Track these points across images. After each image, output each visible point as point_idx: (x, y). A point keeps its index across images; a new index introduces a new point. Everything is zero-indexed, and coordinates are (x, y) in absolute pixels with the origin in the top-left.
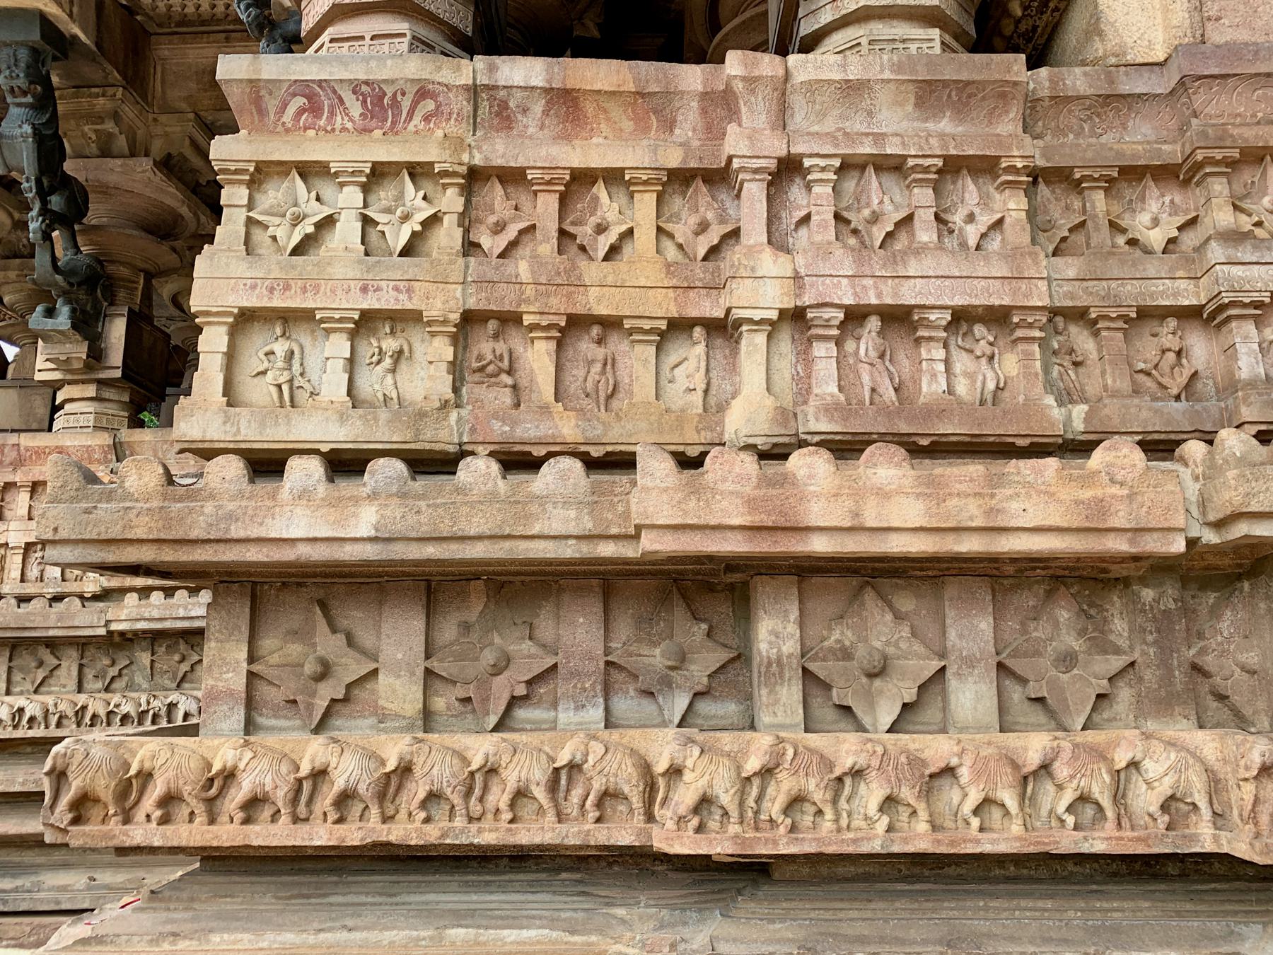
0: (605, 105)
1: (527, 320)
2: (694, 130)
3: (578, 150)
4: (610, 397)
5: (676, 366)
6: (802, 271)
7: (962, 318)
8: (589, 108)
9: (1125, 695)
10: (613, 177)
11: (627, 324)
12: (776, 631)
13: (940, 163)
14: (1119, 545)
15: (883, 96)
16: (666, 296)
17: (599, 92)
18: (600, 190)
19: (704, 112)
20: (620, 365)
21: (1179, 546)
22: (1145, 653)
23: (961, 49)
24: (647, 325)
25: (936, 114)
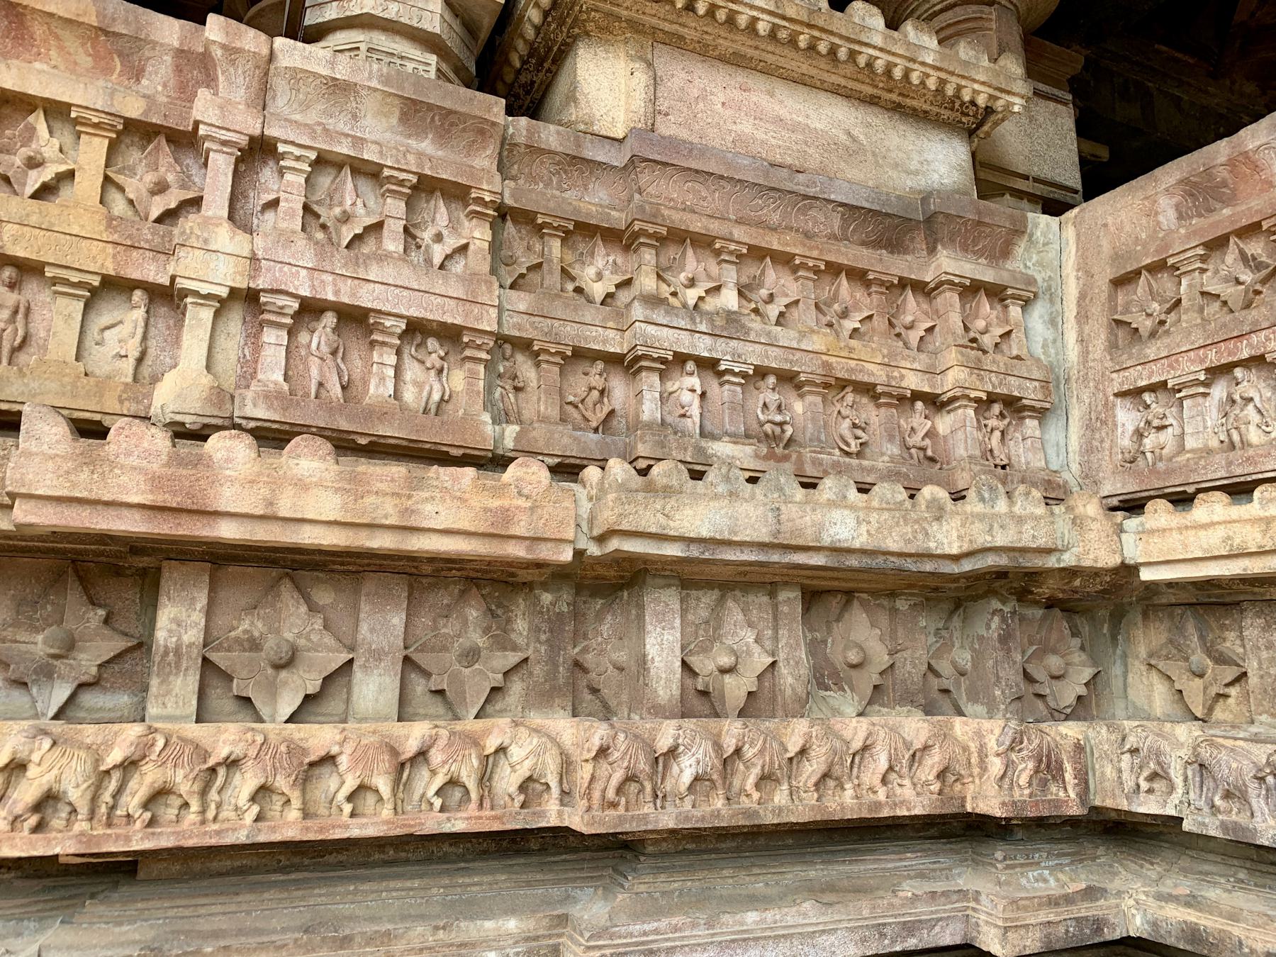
0: (59, 32)
2: (165, 86)
3: (14, 71)
4: (15, 350)
5: (108, 328)
6: (260, 254)
7: (416, 329)
8: (38, 30)
9: (517, 687)
10: (57, 111)
11: (49, 272)
12: (179, 619)
13: (415, 180)
14: (517, 551)
15: (369, 104)
16: (104, 250)
17: (51, 15)
18: (39, 121)
19: (178, 70)
20: (36, 316)
21: (567, 555)
22: (536, 651)
23: (457, 80)
24: (75, 277)
25: (420, 133)
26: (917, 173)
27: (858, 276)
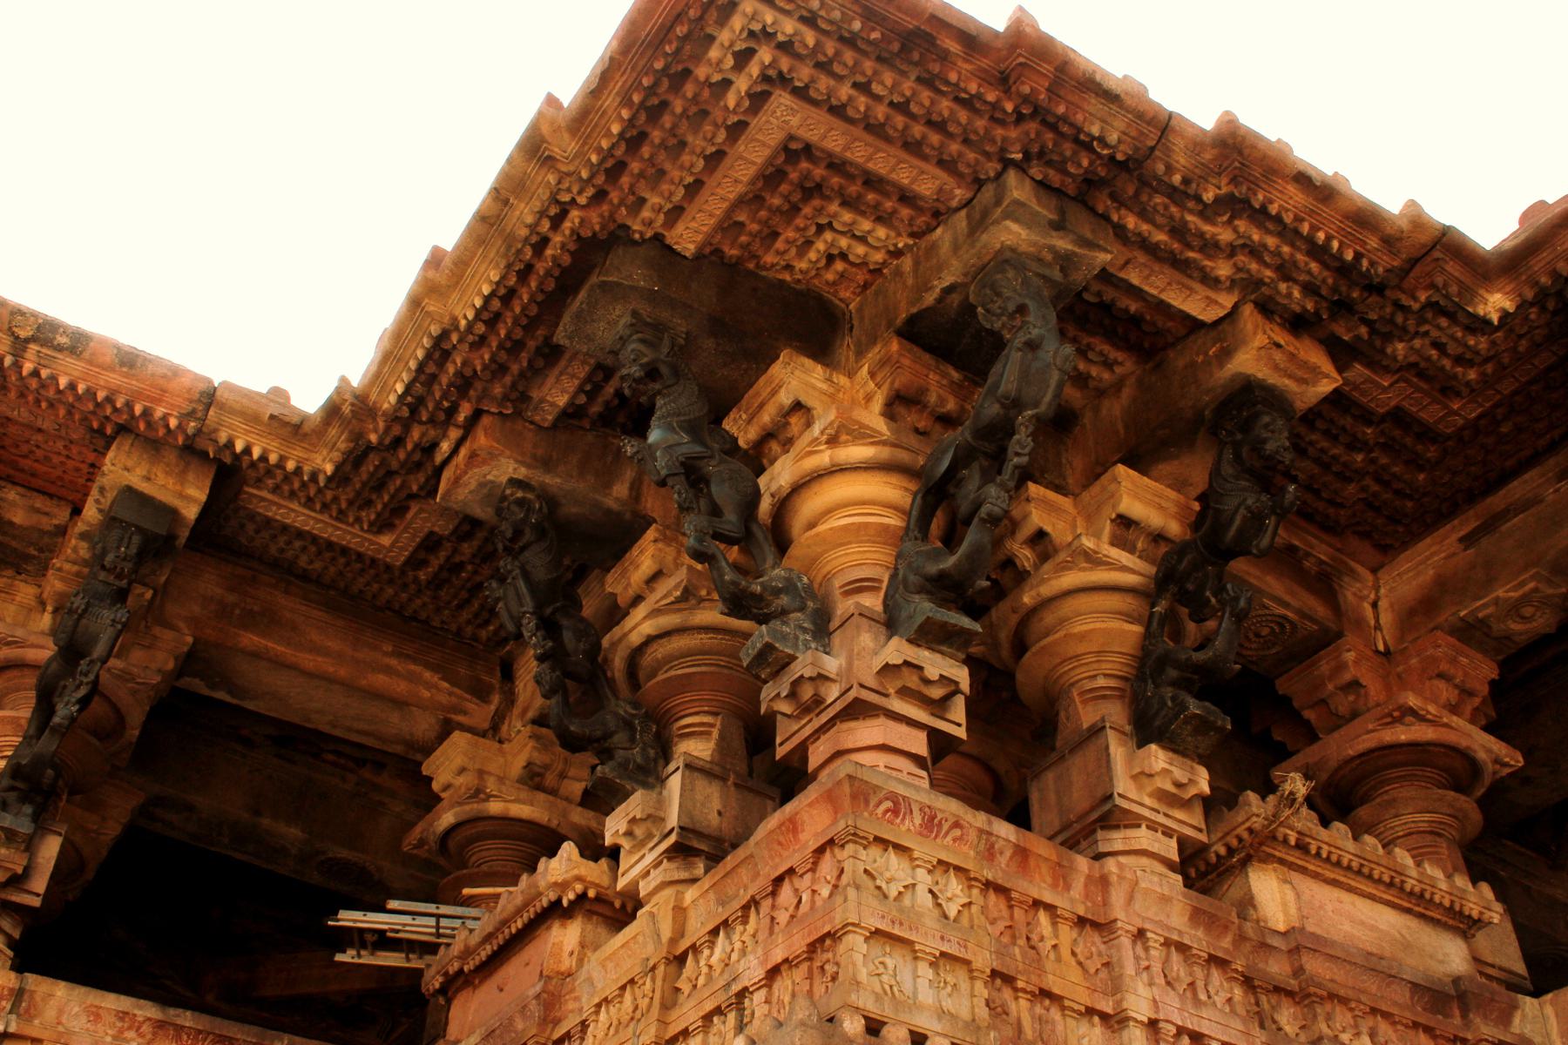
1: (1020, 984)
8: (1032, 862)
10: (1051, 908)
19: (1086, 886)
24: (1076, 1007)
26: (1441, 962)
27: (1428, 1030)
